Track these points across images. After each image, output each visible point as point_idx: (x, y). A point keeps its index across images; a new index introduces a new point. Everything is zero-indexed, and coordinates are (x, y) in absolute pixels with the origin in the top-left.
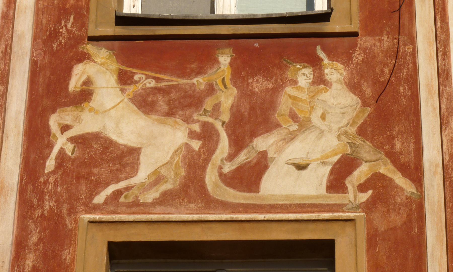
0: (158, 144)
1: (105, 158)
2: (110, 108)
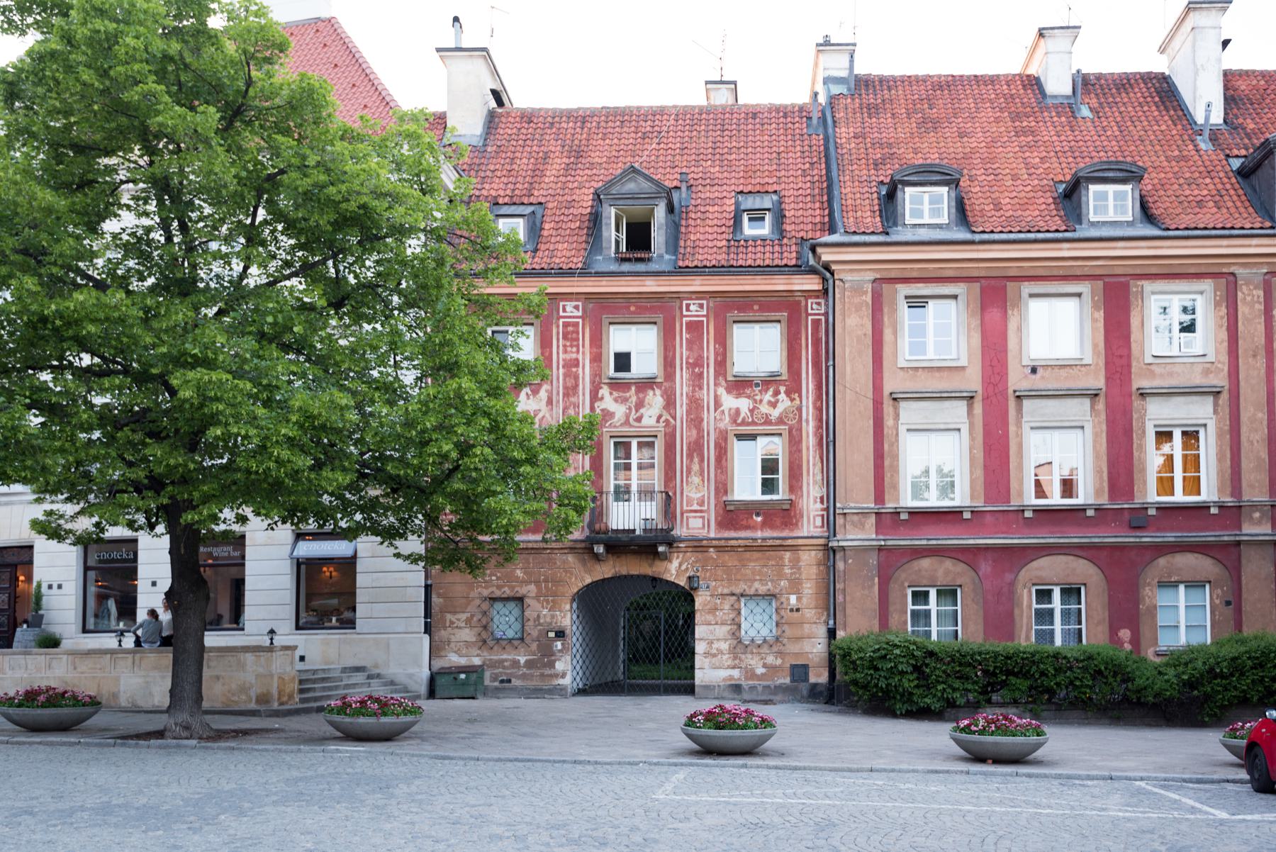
0: (619, 411)
1: (607, 415)
2: (608, 401)
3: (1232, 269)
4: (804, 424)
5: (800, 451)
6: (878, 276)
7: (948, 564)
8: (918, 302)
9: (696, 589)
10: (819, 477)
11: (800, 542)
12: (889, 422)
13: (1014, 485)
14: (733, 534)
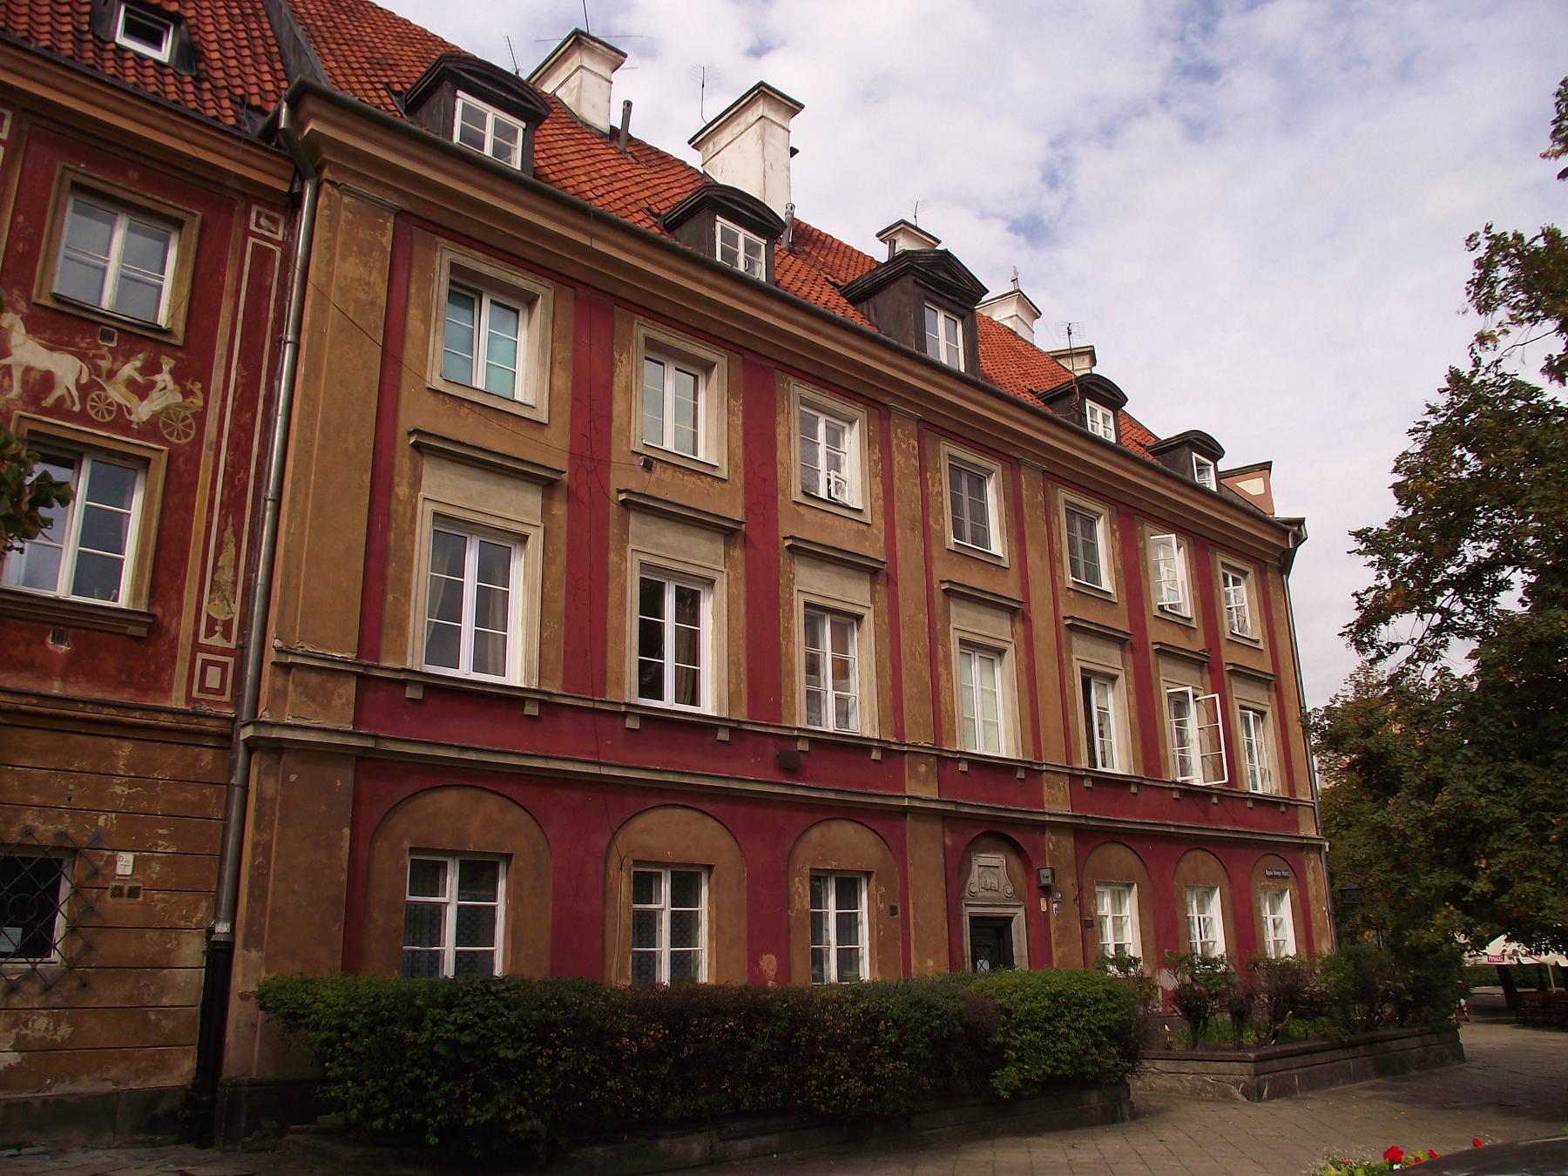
3: (886, 400)
4: (206, 456)
5: (190, 509)
6: (407, 207)
7: (491, 804)
8: (466, 292)
10: (226, 576)
11: (165, 720)
12: (402, 490)
13: (612, 662)
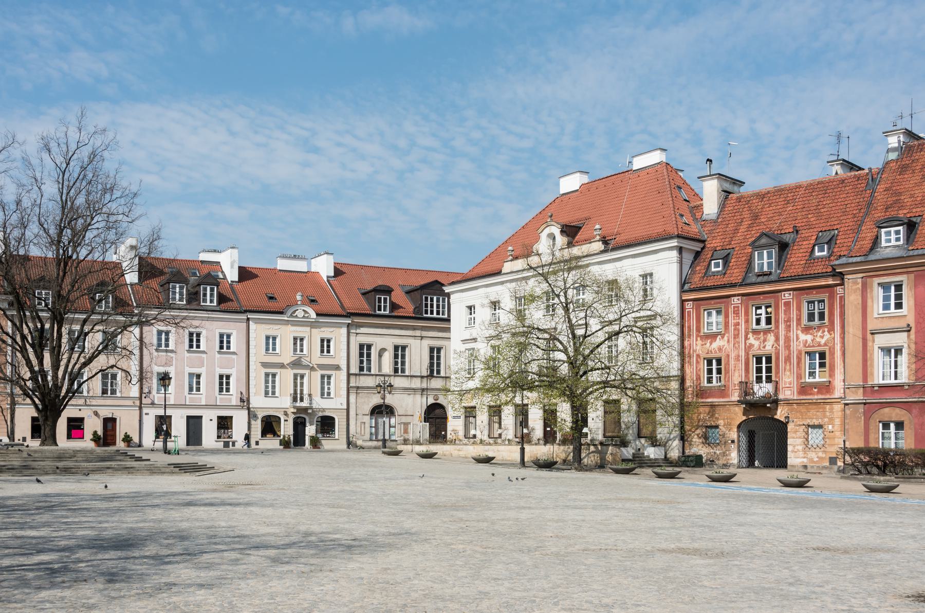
1: (751, 345)
2: (752, 340)
7: (898, 410)
9: (788, 422)
12: (870, 344)
14: (804, 397)
